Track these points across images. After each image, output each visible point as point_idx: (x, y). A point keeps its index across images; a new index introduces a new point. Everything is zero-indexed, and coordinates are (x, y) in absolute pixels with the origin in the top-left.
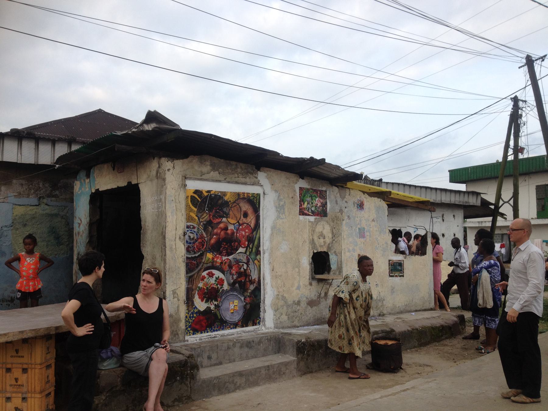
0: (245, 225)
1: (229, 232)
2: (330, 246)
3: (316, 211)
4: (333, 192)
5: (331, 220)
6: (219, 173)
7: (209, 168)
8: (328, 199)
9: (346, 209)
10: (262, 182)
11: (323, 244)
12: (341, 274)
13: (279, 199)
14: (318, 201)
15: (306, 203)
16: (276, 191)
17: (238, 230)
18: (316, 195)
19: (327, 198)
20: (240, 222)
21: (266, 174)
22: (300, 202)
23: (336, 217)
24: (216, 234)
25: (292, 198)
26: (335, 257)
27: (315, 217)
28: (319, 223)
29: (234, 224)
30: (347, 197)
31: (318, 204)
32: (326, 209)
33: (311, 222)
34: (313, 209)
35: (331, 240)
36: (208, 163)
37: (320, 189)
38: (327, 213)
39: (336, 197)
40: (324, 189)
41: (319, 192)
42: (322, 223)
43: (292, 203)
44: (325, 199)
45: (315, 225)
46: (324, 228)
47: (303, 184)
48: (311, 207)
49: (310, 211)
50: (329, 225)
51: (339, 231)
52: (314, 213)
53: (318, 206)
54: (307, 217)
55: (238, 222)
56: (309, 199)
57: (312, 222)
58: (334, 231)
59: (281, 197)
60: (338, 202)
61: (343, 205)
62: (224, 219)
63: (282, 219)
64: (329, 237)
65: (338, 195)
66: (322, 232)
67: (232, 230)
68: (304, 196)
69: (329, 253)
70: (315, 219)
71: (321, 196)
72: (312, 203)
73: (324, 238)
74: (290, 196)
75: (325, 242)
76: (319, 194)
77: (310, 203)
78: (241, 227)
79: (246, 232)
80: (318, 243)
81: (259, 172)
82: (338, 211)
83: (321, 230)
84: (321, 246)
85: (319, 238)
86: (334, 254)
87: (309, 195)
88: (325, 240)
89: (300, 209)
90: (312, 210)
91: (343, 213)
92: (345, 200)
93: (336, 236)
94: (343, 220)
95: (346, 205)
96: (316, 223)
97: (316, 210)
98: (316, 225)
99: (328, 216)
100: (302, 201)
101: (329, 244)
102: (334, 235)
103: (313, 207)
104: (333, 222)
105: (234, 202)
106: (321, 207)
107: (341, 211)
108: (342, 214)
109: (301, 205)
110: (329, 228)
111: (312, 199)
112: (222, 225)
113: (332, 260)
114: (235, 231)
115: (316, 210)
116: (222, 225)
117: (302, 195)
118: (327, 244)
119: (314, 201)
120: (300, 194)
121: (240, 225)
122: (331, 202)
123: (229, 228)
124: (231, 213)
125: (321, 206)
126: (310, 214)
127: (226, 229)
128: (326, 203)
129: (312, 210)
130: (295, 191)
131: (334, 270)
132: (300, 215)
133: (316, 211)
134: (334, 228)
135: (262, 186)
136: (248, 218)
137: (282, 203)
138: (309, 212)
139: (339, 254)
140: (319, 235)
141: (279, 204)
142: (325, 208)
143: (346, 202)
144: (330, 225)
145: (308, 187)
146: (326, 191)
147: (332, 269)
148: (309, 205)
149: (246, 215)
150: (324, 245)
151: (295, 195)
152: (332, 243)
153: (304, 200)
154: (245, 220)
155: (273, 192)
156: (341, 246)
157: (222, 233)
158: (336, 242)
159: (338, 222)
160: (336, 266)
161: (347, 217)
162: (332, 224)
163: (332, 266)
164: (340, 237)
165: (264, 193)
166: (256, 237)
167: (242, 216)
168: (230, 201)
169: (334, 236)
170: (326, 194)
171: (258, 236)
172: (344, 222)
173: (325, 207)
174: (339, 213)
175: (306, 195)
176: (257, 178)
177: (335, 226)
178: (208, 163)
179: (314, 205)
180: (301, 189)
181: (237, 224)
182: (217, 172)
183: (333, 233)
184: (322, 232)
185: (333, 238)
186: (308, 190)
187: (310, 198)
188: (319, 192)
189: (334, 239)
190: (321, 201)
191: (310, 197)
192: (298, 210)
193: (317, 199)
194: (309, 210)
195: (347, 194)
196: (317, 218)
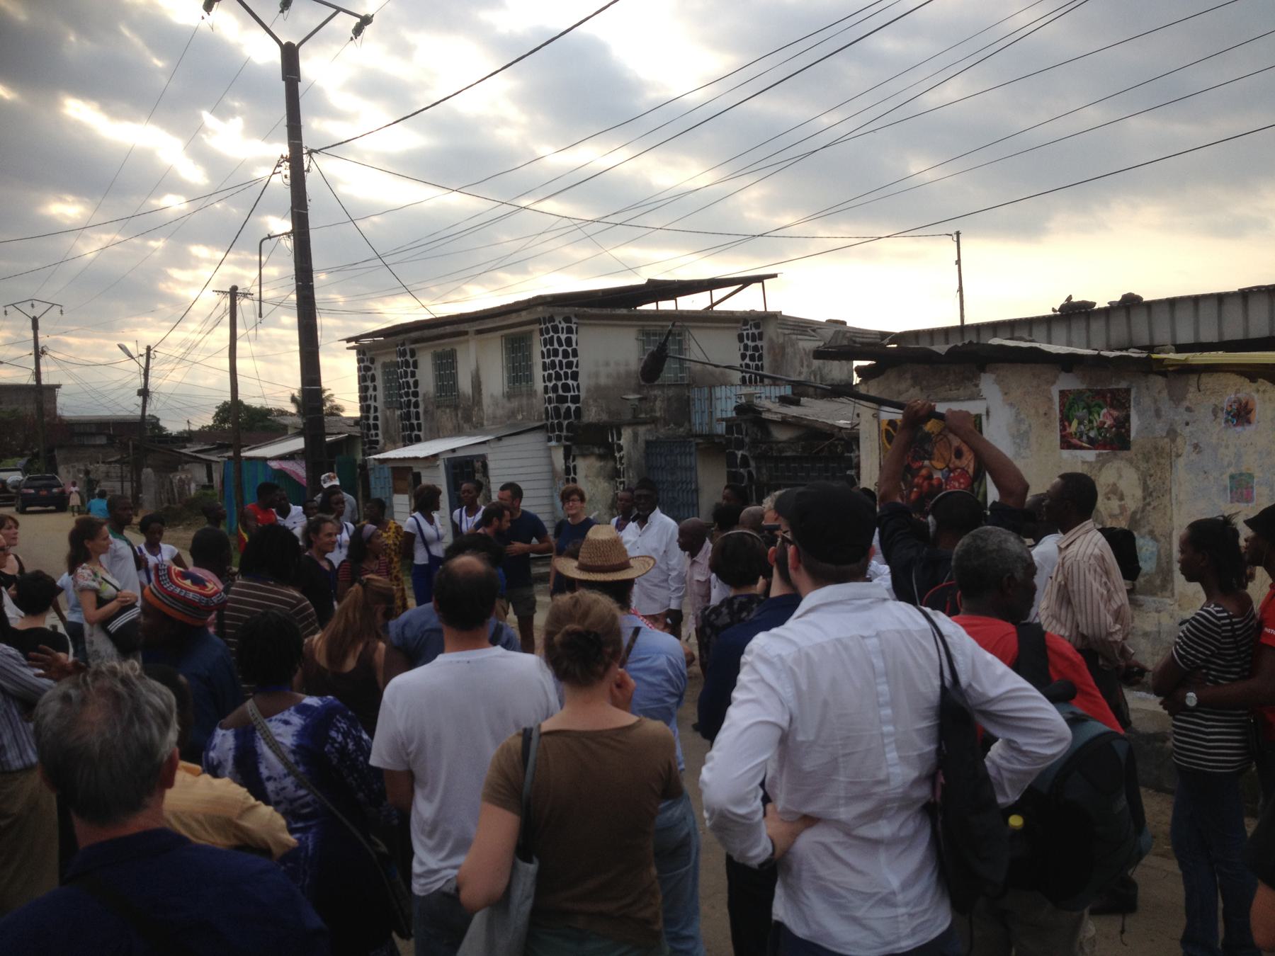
0: (959, 470)
1: (935, 482)
2: (1138, 516)
3: (1100, 438)
4: (1148, 389)
5: (1140, 456)
6: (922, 389)
7: (909, 382)
8: (1132, 409)
9: (1188, 429)
10: (984, 393)
11: (1117, 511)
12: (1170, 587)
13: (1019, 421)
14: (1105, 417)
15: (1075, 423)
16: (1011, 405)
17: (947, 479)
18: (1101, 402)
19: (1129, 407)
20: (951, 466)
21: (993, 376)
22: (1062, 420)
23: (1156, 448)
24: (918, 486)
25: (1045, 414)
26: (1151, 543)
27: (1097, 452)
28: (1108, 465)
29: (941, 470)
30: (1190, 396)
31: (1105, 423)
32: (1128, 431)
33: (1087, 462)
34: (1092, 434)
35: (1140, 505)
36: (908, 376)
37: (1114, 386)
38: (1129, 442)
39: (1155, 401)
40: (1123, 385)
41: (1109, 395)
42: (1117, 464)
43: (1046, 426)
44: (1126, 408)
45: (1097, 468)
46: (1120, 476)
47: (1069, 382)
48: (1089, 430)
49: (1085, 438)
50: (1134, 470)
51: (1164, 483)
52: (1093, 444)
53: (1106, 426)
54: (1078, 452)
55: (947, 466)
56: (1082, 413)
57: (1091, 462)
58: (1149, 482)
59: (1022, 416)
60: (1163, 413)
61: (1177, 418)
62: (926, 462)
63: (1023, 458)
64: (1133, 495)
65: (1165, 394)
66: (1115, 484)
67: (939, 479)
68: (1070, 409)
69: (1136, 534)
70: (1098, 456)
71: (1115, 402)
72: (1091, 422)
73: (1121, 498)
74: (1041, 412)
75: (1123, 509)
76: (1108, 400)
77: (1086, 422)
78: (952, 475)
79: (960, 483)
80: (1106, 509)
81: (982, 374)
82: (1164, 434)
83: (1111, 481)
84: (1112, 516)
85: (1109, 499)
86: (1148, 537)
87: (1082, 404)
88: (1123, 502)
89: (1062, 437)
90: (1088, 437)
91: (1179, 440)
92: (1186, 403)
93: (1154, 494)
94: (1178, 456)
95: (1186, 417)
96: (1099, 465)
97: (1100, 435)
98: (1100, 470)
99: (1133, 448)
100: (1065, 419)
101: (1135, 513)
102: (1147, 493)
103: (1092, 428)
104: (1147, 462)
105: (940, 433)
106: (1114, 429)
107: (1172, 434)
108: (1173, 441)
109: (1063, 428)
110: (1136, 476)
111: (1090, 413)
112: (924, 472)
113: (1144, 550)
114: (943, 480)
115: (1100, 435)
116: (924, 472)
117: (1064, 407)
118: (1129, 513)
119: (1096, 416)
120: (1062, 405)
121: (951, 471)
122: (1141, 414)
123: (935, 476)
124: (935, 451)
125: (1114, 426)
126: (1084, 444)
127: (930, 477)
128: (1127, 418)
129: (1088, 437)
130: (1051, 400)
131: (1147, 574)
132: (1062, 448)
133: (1100, 438)
134: (1151, 476)
135: (985, 399)
136: (964, 458)
137: (1024, 427)
138: (1082, 442)
139: (1163, 540)
140: (1108, 490)
141: (1018, 430)
142: (1123, 430)
143: (1189, 409)
144: (1137, 468)
145: (1082, 387)
146: (1128, 391)
147: (1143, 572)
148: (1082, 427)
149: (959, 454)
150: (1121, 514)
151: (1050, 408)
152: (1143, 510)
153: (1071, 417)
154: (957, 463)
155: (1007, 407)
156: (1171, 519)
157: (926, 483)
158: (1154, 508)
159: (1162, 461)
160: (1154, 566)
161: (1188, 448)
162: (1143, 466)
163: (1141, 564)
164: (1168, 497)
165: (988, 413)
166: (978, 493)
167: (953, 457)
168: (933, 433)
169: (1151, 495)
170: (1129, 395)
171: (982, 490)
172: (1181, 462)
173: (1123, 426)
174: (1166, 440)
175: (1076, 406)
176: (977, 386)
177: (1152, 472)
178: (908, 376)
179: (1095, 424)
180: (1062, 393)
181: (946, 469)
182: (918, 388)
183: (1145, 488)
184: (1115, 484)
185: (1144, 499)
186: (1080, 392)
187: (1085, 411)
188: (1109, 395)
189: (1148, 500)
190: (1115, 413)
191: (1084, 408)
192: (1059, 437)
193: (1105, 411)
194: (1081, 436)
195: (1192, 389)
196: (1102, 454)
